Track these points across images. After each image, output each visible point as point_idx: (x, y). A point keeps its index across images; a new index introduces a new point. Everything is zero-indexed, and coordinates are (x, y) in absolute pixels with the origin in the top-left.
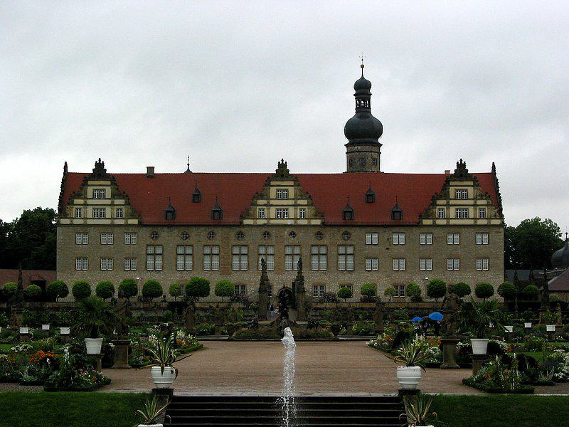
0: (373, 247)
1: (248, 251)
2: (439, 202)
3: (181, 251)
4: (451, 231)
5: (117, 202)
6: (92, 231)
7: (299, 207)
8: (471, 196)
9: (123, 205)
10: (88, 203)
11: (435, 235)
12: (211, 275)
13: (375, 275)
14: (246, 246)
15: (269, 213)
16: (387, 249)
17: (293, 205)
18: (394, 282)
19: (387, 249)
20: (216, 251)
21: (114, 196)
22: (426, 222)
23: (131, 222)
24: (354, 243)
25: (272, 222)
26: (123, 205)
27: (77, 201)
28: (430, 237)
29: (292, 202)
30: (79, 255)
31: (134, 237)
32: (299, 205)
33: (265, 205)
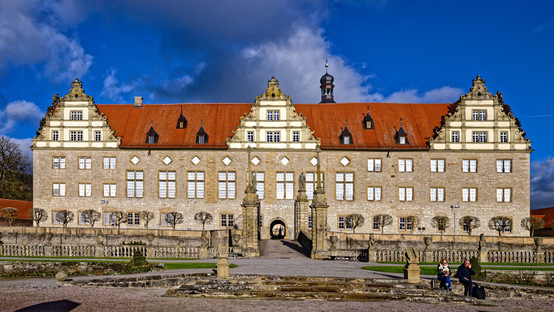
0: (376, 174)
1: (236, 178)
2: (452, 124)
3: (163, 176)
4: (467, 157)
5: (94, 124)
6: (68, 154)
7: (292, 130)
8: (491, 116)
9: (102, 127)
10: (64, 125)
11: (447, 162)
12: (195, 203)
13: (378, 205)
14: (234, 172)
15: (258, 137)
16: (393, 176)
17: (286, 128)
18: (400, 213)
19: (393, 176)
20: (200, 176)
21: (91, 119)
22: (437, 146)
23: (109, 145)
24: (355, 170)
25: (262, 146)
26: (102, 127)
27: (53, 123)
28: (441, 163)
29: (284, 124)
30: (55, 181)
31: (113, 160)
32: (292, 127)
33: (255, 127)
